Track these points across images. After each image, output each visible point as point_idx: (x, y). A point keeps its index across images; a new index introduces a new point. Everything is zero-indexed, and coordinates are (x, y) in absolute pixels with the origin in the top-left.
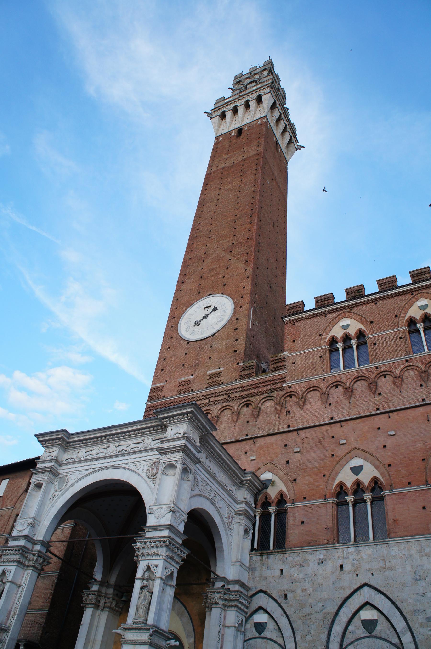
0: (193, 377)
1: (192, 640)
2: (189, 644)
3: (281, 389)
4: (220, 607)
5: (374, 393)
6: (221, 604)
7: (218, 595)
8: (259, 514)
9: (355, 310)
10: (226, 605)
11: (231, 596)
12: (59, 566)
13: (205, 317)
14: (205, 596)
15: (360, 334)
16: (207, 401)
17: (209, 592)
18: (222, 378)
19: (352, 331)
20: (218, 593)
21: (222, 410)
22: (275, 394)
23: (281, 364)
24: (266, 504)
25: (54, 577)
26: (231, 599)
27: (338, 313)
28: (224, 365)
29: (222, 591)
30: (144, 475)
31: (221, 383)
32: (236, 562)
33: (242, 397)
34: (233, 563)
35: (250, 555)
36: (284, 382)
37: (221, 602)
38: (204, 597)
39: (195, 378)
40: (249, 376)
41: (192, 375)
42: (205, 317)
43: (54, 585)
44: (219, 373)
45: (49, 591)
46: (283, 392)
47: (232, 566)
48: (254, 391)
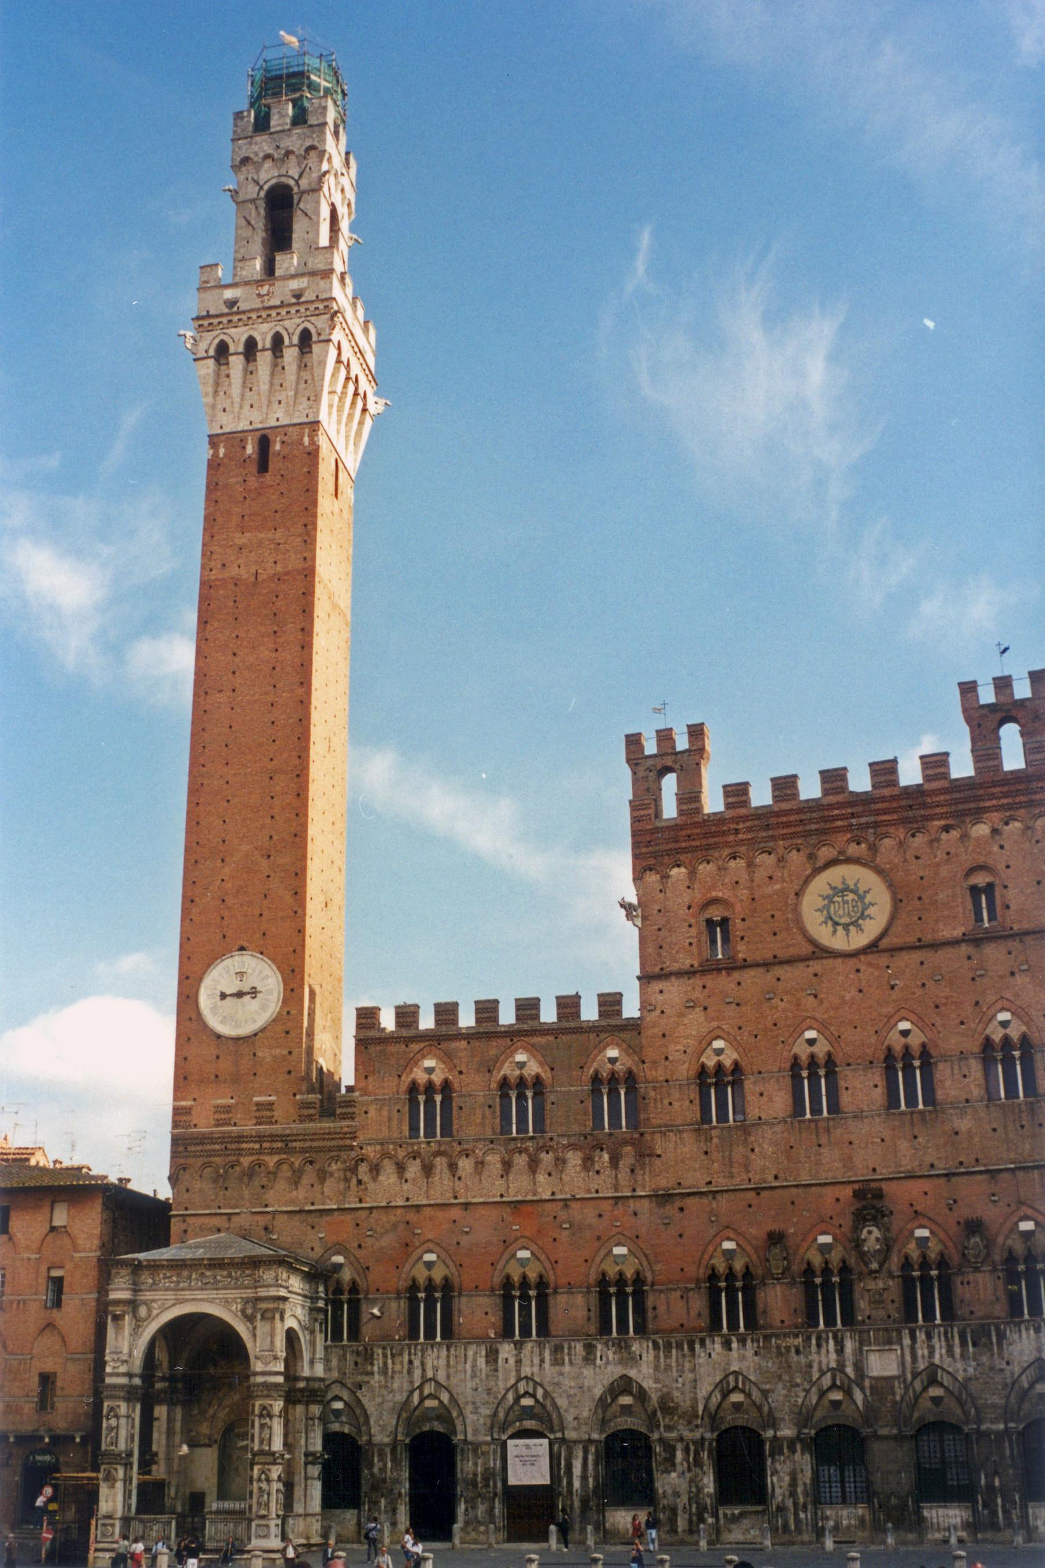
0: (232, 1101)
3: (351, 1148)
5: (454, 1176)
9: (444, 1045)
13: (240, 995)
15: (446, 1086)
16: (257, 1146)
18: (275, 1113)
19: (437, 1078)
21: (279, 1164)
22: (344, 1155)
23: (349, 1110)
24: (339, 1291)
27: (422, 1045)
28: (277, 1093)
30: (239, 1313)
31: (273, 1120)
33: (304, 1151)
36: (354, 1138)
39: (237, 1104)
40: (310, 1118)
41: (232, 1098)
42: (240, 995)
44: (271, 1104)
46: (353, 1154)
48: (321, 1144)
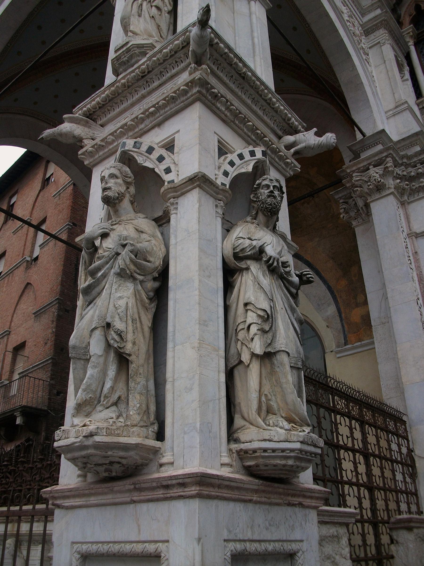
1: (332, 310)
2: (327, 320)
4: (392, 193)
6: (393, 186)
7: (380, 170)
8: (411, 37)
10: (404, 189)
11: (410, 169)
12: (57, 290)
14: (340, 198)
17: (354, 171)
20: (375, 166)
25: (53, 309)
26: (413, 174)
29: (387, 157)
32: (396, 107)
34: (391, 112)
35: (421, 107)
37: (391, 183)
38: (341, 201)
43: (55, 319)
45: (50, 331)
47: (392, 120)
